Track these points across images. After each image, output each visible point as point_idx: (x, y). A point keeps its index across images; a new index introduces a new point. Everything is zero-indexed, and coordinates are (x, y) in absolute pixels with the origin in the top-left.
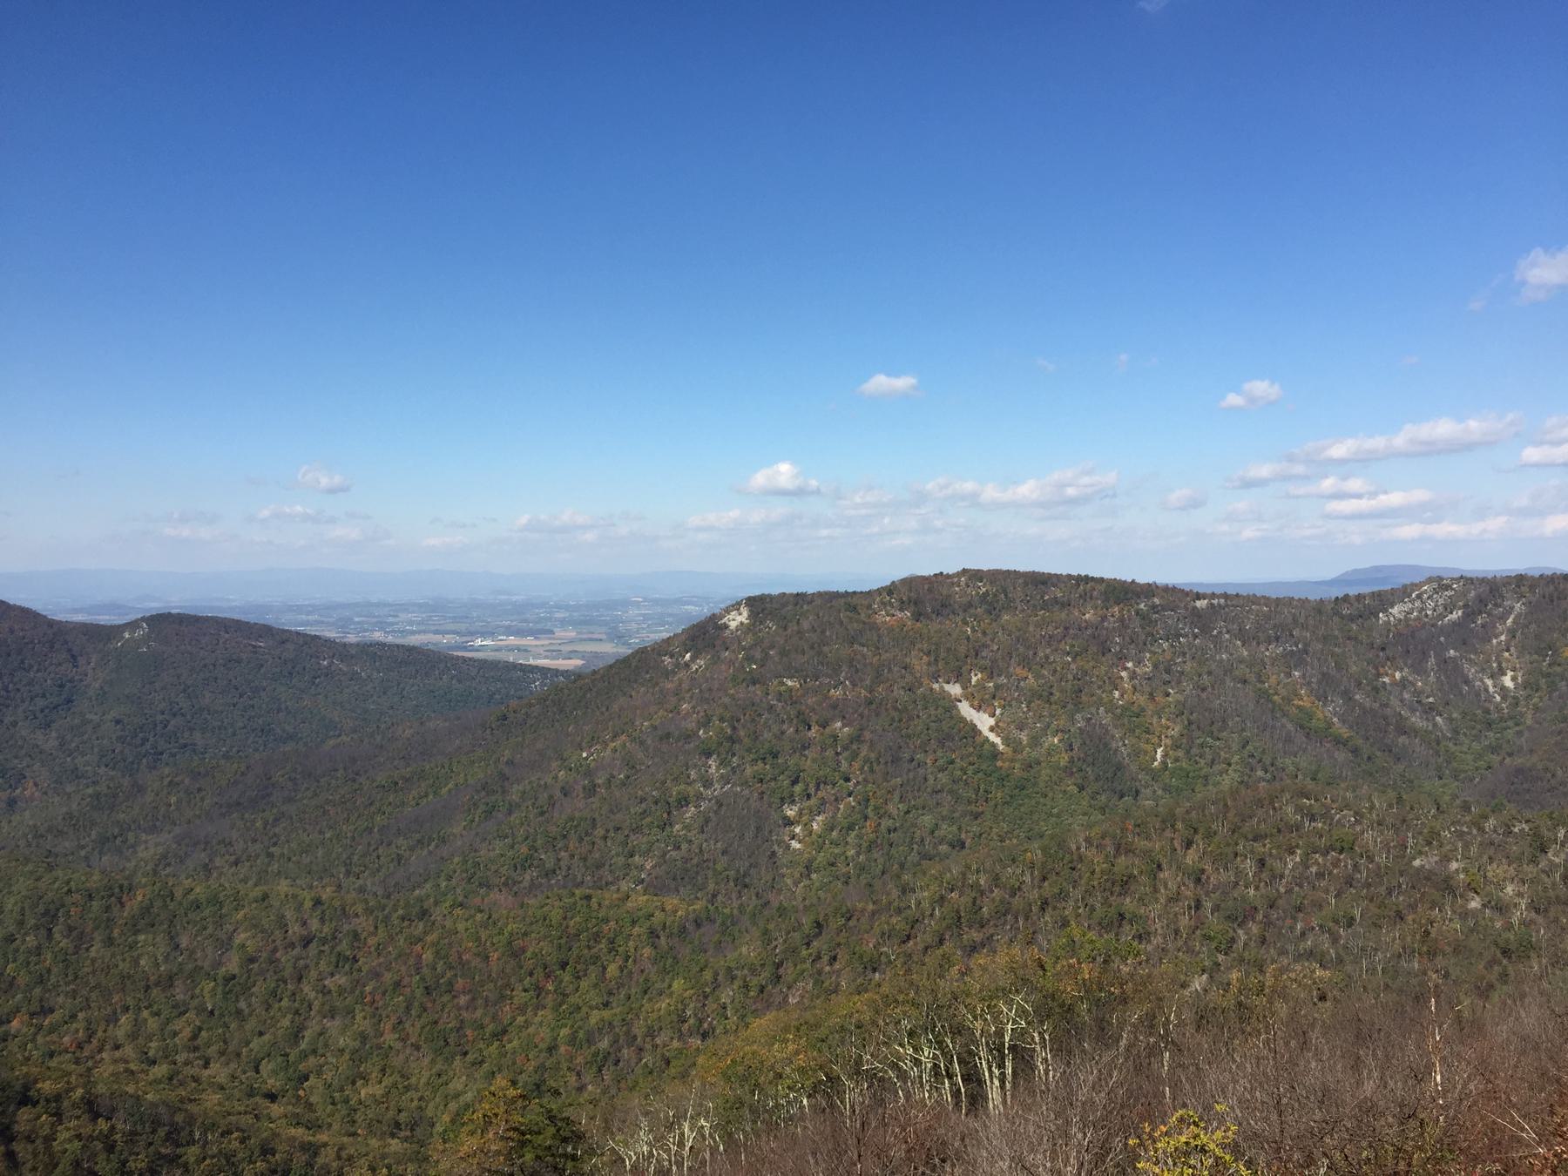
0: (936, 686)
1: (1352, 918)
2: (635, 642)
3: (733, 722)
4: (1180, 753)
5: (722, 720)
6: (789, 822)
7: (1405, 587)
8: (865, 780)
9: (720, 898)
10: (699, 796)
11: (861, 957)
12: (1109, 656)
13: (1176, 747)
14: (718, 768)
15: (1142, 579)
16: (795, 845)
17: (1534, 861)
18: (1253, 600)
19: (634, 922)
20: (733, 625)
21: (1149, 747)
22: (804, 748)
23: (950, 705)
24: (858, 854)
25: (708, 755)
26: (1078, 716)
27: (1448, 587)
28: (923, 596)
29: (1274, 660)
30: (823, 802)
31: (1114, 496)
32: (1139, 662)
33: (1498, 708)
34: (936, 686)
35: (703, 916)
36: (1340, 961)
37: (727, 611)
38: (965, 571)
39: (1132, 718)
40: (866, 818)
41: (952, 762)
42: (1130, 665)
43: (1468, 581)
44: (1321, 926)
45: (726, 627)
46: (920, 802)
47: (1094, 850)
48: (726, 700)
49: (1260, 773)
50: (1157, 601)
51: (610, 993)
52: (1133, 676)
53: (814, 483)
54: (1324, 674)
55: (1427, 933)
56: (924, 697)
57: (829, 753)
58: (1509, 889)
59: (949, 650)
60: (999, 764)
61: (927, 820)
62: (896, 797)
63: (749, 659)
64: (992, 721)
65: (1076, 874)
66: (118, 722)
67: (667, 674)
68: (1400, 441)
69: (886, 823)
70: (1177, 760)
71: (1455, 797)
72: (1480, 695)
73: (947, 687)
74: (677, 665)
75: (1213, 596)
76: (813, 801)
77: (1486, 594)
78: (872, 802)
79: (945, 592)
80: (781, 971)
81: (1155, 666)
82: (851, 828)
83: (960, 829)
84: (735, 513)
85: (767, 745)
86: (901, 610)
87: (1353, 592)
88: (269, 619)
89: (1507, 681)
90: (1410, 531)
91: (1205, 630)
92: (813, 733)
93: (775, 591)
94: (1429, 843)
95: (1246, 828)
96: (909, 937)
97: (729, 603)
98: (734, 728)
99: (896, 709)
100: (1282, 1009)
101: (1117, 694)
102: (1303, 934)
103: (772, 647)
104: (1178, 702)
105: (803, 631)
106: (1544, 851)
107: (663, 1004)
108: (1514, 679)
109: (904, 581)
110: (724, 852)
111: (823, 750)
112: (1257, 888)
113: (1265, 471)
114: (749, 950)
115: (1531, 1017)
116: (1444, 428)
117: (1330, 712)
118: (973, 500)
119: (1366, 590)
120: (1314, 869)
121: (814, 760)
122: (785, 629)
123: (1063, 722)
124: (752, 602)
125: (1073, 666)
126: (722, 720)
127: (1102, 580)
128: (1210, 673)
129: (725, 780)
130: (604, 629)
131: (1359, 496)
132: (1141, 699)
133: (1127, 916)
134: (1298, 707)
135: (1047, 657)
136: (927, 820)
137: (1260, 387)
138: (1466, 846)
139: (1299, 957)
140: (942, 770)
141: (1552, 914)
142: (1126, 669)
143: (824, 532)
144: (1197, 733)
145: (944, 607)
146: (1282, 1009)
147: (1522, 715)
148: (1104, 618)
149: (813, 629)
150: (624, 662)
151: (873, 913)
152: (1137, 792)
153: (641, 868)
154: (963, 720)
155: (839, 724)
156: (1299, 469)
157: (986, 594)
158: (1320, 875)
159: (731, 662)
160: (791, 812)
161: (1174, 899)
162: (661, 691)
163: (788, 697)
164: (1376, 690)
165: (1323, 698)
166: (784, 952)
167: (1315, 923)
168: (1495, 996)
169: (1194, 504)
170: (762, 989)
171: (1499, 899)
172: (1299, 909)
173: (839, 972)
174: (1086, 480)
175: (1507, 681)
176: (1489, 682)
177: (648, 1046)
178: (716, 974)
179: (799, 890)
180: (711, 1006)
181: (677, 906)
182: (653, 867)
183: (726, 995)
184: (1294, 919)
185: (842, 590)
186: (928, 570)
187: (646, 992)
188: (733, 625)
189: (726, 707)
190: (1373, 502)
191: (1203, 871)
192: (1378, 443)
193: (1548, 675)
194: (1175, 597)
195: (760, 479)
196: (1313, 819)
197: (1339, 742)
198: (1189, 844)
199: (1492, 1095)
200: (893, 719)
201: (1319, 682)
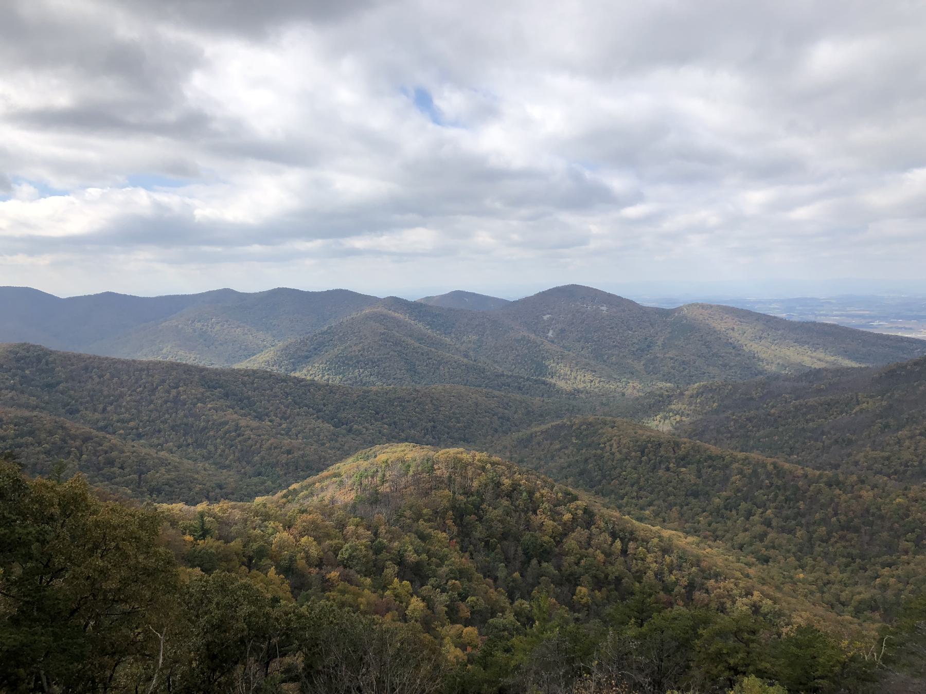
66: (672, 359)
88: (748, 307)
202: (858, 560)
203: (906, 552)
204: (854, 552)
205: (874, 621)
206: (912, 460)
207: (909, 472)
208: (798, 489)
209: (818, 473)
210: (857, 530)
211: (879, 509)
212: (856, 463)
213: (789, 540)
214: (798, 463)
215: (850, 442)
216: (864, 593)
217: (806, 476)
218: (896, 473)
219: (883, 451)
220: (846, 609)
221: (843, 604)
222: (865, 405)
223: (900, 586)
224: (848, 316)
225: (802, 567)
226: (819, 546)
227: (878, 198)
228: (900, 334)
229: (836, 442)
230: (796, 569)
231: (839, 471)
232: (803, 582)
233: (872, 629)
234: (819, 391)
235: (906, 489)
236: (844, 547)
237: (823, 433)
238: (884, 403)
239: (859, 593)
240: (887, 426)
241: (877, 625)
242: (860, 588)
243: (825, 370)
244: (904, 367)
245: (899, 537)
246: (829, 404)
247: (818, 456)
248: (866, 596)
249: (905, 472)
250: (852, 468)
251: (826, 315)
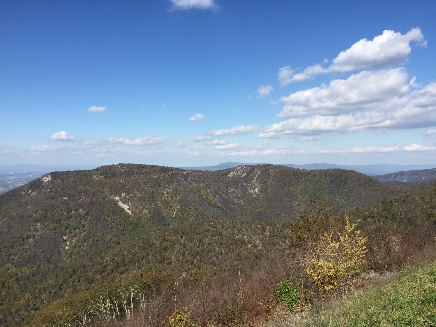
0: (112, 197)
1: (222, 253)
2: (11, 187)
3: (46, 211)
4: (180, 213)
5: (42, 211)
6: (65, 241)
7: (233, 167)
8: (89, 226)
9: (41, 266)
10: (34, 235)
11: (88, 279)
12: (161, 187)
13: (179, 211)
14: (40, 226)
15: (169, 166)
16: (67, 248)
17: (262, 234)
18: (198, 171)
19: (11, 277)
20: (46, 181)
21: (172, 212)
22: (70, 218)
23: (116, 203)
24: (87, 248)
25: (37, 222)
26: (152, 204)
27: (243, 168)
28: (107, 171)
29: (203, 187)
30: (76, 234)
31: (162, 143)
32: (169, 189)
33: (254, 197)
34: (112, 197)
35: (36, 273)
36: (219, 264)
37: (44, 177)
39: (166, 204)
40: (90, 238)
41: (116, 219)
42: (166, 189)
43: (247, 166)
44: (215, 256)
45: (43, 182)
46: (106, 231)
47: (157, 241)
48: (43, 204)
49: (200, 217)
50: (174, 172)
51: (3, 300)
52: (167, 192)
53: (73, 138)
54: (215, 190)
55: (239, 254)
56: (108, 201)
57: (78, 219)
58: (257, 242)
59: (115, 187)
60: (130, 219)
61: (109, 237)
62: (99, 231)
63: (51, 191)
64: (128, 207)
65: (152, 248)
67: (22, 197)
68: (232, 131)
69: (96, 239)
70: (179, 215)
71: (245, 220)
72: (250, 194)
73: (115, 198)
74: (26, 194)
75: (188, 170)
76: (73, 234)
77: (251, 169)
78: (92, 233)
79: (114, 170)
80: (62, 287)
81: (173, 190)
82: (85, 241)
83: (119, 238)
84: (46, 146)
85: (57, 218)
86: (101, 175)
87: (222, 169)
89: (256, 191)
90: (234, 154)
91: (186, 179)
92: (73, 213)
93: (60, 170)
94: (239, 232)
95: (196, 232)
96: (103, 272)
97: (44, 174)
98: (46, 213)
99: (99, 205)
100: (204, 279)
101: (163, 198)
102: (210, 258)
103: (59, 187)
104: (179, 199)
105: (69, 183)
106: (265, 232)
107: (22, 302)
108: (258, 190)
109: (102, 167)
110: (42, 252)
111: (76, 218)
112: (199, 247)
113: (200, 137)
114: (51, 281)
115: (262, 273)
116: (242, 128)
117: (216, 200)
118: (122, 144)
119: (225, 168)
120: (213, 241)
121: (73, 221)
122: (63, 182)
123: (148, 206)
124: (52, 174)
125: (151, 190)
126: (42, 211)
127: (159, 166)
128: (187, 191)
129: (43, 229)
131: (223, 145)
132: (170, 199)
133: (166, 258)
134: (209, 199)
135: (144, 188)
136: (109, 237)
137: (199, 116)
138: (248, 232)
139: (209, 265)
140: (113, 222)
141: (266, 247)
142: (165, 191)
143: (76, 153)
144: (184, 207)
145: (114, 174)
146: (204, 279)
147: (259, 199)
148: (160, 177)
149: (73, 182)
150: (7, 193)
151: (92, 266)
152: (169, 224)
153: (14, 259)
154: (119, 207)
155: (81, 210)
156: (209, 137)
157: (126, 171)
158: (214, 242)
159: (45, 193)
160: (65, 238)
161: (178, 253)
162: (20, 203)
163: (65, 202)
164: (227, 194)
165: (215, 196)
166: (63, 281)
167: (213, 255)
168: (255, 269)
169: (183, 146)
170: (56, 293)
171: (255, 245)
172: (209, 252)
173: (81, 285)
174: (154, 139)
175: (256, 191)
176: (252, 191)
177: (16, 315)
178: (40, 291)
179: (68, 261)
180: (38, 300)
181: (26, 270)
182: (18, 259)
183: (43, 296)
184: (208, 254)
185: (82, 170)
187: (15, 299)
188: (46, 181)
189: (43, 207)
190: (226, 146)
191: (186, 244)
192: (227, 131)
193: (265, 189)
194: (178, 171)
195: (55, 136)
196: (212, 228)
197: (219, 207)
198: (182, 237)
199: (253, 294)
200: (98, 208)
201: (214, 192)
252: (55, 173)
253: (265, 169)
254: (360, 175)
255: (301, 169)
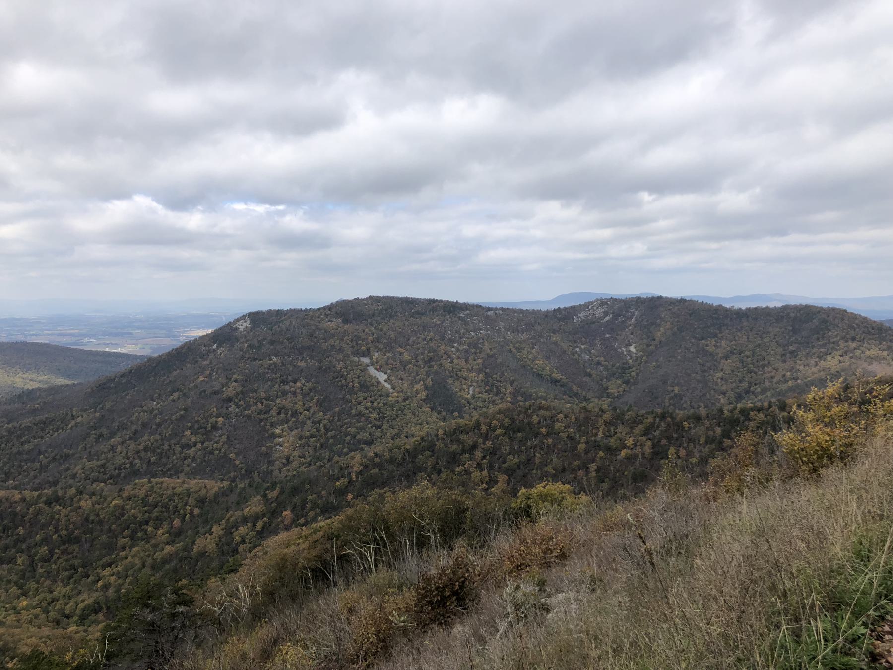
15: (461, 301)
18: (514, 311)
20: (241, 328)
28: (347, 311)
38: (370, 297)
43: (614, 300)
45: (237, 329)
60: (390, 398)
64: (386, 376)
75: (496, 309)
89: (632, 349)
93: (265, 309)
127: (441, 301)
130: (164, 331)
154: (371, 377)
157: (382, 309)
185: (303, 308)
186: (350, 297)
188: (241, 328)
197: (555, 382)
202: (80, 570)
203: (124, 549)
204: (76, 562)
205: (97, 622)
206: (124, 463)
207: (122, 475)
208: (15, 514)
209: (36, 494)
210: (77, 540)
211: (98, 515)
212: (74, 476)
213: (10, 571)
214: (15, 488)
215: (67, 457)
216: (87, 599)
217: (24, 500)
218: (110, 478)
219: (98, 459)
220: (71, 620)
221: (68, 617)
222: (79, 419)
223: (120, 581)
224: (59, 335)
225: (25, 594)
226: (41, 567)
227: (82, 224)
228: (107, 350)
229: (54, 459)
230: (18, 598)
231: (59, 487)
232: (26, 609)
233: (95, 632)
234: (34, 412)
235: (120, 490)
236: (67, 561)
237: (40, 453)
238: (97, 415)
239: (83, 601)
240: (101, 436)
241: (101, 626)
242: (84, 596)
243: (39, 389)
244: (111, 380)
245: (116, 537)
246: (44, 423)
247: (35, 477)
248: (90, 601)
249: (119, 475)
250: (71, 482)
251: (37, 335)
252: (258, 313)
253: (652, 306)
254: (854, 317)
255: (727, 305)
